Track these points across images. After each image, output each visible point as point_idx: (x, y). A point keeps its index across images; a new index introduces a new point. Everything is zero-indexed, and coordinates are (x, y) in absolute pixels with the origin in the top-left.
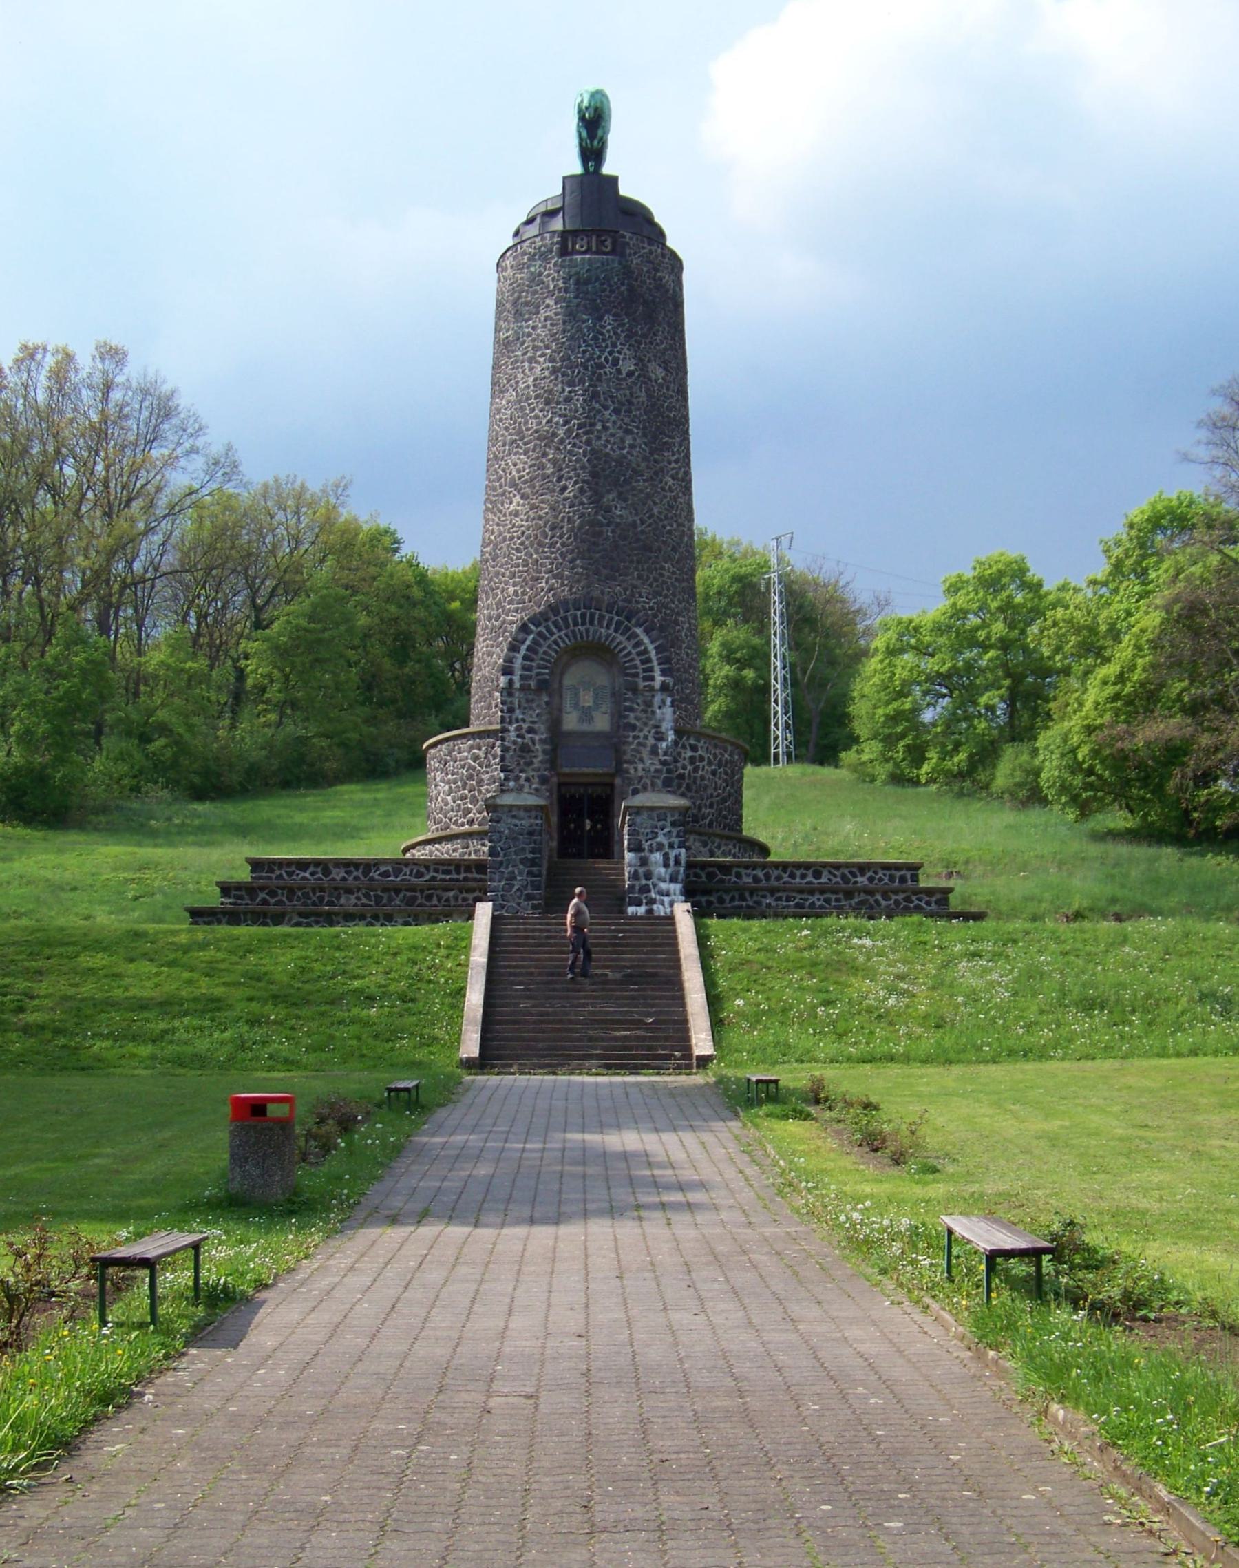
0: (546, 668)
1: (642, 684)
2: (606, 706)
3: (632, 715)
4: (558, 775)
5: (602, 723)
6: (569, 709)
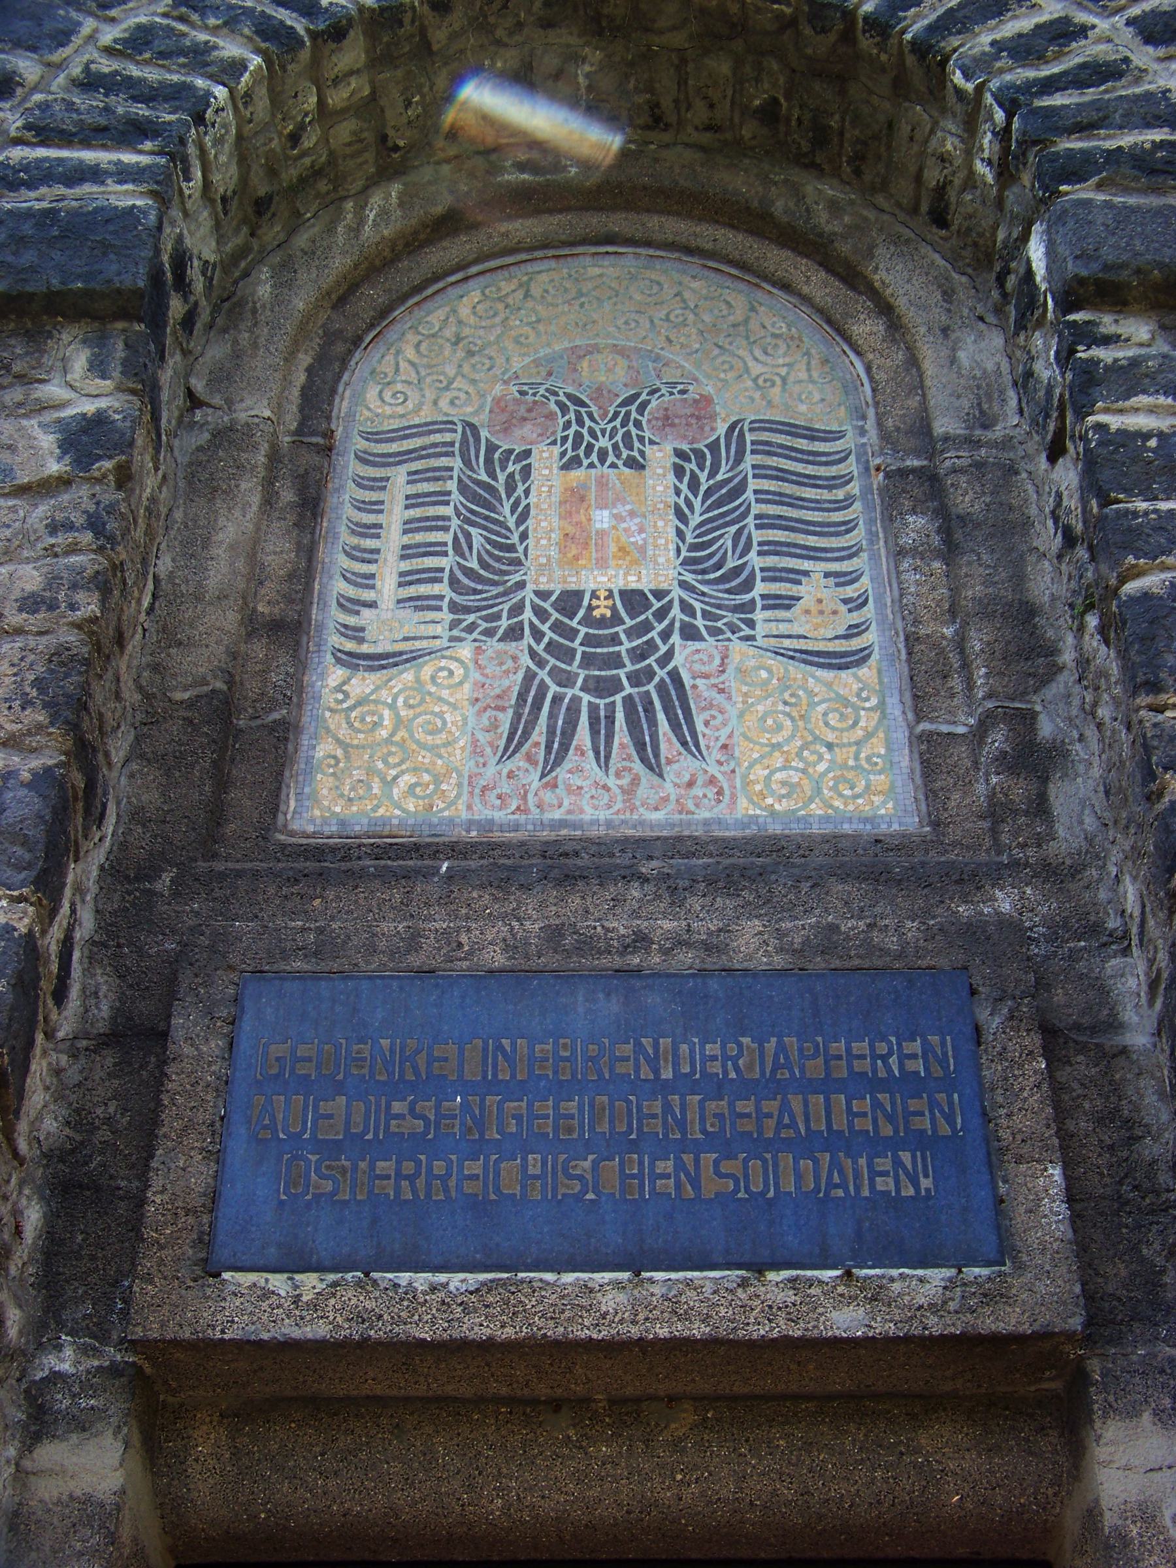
0: (133, 132)
2: (850, 588)
4: (168, 1390)
6: (386, 625)
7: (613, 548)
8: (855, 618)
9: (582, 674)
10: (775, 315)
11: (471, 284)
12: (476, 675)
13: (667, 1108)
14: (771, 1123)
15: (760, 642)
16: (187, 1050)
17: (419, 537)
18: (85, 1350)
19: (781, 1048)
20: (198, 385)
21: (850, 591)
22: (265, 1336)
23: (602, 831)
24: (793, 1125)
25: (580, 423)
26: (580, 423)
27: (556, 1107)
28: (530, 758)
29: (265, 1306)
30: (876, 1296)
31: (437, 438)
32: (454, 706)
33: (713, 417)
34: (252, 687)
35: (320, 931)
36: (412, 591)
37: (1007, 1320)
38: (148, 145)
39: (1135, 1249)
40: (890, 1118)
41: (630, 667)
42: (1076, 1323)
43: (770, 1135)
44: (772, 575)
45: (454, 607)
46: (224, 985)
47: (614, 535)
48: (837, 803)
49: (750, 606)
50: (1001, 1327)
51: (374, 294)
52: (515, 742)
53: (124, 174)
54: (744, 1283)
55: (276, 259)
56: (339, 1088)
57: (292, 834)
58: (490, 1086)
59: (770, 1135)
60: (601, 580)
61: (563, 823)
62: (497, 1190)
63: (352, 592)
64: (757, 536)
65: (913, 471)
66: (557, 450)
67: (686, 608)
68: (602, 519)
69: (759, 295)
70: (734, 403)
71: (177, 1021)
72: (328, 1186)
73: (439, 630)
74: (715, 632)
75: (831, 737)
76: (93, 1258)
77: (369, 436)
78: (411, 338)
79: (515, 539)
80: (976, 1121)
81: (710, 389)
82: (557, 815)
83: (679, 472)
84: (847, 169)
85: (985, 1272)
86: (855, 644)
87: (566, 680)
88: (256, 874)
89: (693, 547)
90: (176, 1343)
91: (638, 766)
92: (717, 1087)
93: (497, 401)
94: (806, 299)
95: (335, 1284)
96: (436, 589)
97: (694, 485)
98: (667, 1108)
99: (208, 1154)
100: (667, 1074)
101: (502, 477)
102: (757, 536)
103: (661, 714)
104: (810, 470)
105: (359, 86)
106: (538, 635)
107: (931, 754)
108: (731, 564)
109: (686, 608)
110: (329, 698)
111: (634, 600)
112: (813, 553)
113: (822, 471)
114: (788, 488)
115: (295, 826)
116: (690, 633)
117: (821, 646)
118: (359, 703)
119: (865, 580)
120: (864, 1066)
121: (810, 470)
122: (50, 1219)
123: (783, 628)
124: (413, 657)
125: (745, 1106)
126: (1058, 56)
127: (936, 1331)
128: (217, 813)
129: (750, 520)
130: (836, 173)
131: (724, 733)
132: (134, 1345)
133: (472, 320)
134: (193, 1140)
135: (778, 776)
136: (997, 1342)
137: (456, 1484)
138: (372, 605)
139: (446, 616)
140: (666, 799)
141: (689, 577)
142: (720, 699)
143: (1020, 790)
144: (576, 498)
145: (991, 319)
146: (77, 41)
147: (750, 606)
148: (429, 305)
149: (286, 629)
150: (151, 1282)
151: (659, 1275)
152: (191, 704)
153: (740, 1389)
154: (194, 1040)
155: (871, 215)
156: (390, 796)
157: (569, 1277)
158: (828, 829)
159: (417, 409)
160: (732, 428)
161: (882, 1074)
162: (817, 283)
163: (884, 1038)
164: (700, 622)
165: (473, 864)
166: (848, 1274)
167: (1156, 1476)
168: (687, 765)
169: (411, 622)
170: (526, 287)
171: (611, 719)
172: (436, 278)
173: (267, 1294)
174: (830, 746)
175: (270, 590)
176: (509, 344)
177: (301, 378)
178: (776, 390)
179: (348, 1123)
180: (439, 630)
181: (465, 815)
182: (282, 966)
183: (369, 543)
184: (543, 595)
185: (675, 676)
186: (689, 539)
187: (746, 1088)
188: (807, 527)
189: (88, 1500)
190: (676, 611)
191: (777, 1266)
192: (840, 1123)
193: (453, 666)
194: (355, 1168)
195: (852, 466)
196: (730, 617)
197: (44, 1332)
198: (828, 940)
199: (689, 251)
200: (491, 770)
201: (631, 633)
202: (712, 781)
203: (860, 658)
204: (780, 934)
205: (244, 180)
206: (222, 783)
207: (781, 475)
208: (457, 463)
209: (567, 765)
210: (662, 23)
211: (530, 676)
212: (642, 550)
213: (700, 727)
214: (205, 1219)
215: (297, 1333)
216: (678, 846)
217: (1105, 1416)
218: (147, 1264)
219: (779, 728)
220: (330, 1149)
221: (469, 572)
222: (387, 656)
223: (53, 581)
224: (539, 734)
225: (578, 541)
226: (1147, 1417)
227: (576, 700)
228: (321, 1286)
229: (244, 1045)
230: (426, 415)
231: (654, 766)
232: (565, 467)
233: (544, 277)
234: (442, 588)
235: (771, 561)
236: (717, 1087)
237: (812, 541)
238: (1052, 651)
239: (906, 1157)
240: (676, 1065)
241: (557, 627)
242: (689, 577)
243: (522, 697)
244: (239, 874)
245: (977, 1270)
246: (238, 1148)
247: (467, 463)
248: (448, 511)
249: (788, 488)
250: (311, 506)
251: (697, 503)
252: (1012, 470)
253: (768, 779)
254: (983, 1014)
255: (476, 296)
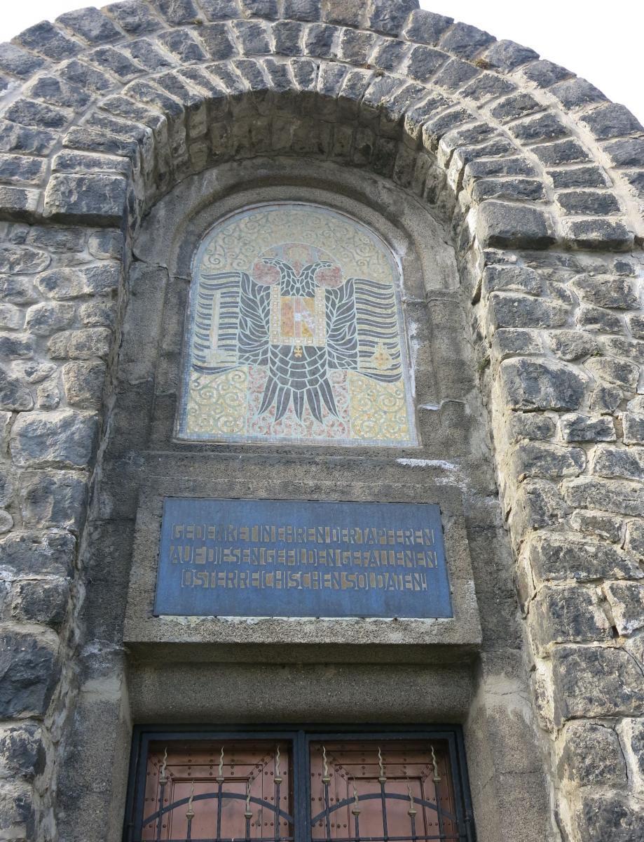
0: (113, 146)
1: (562, 224)
3: (543, 337)
5: (375, 411)
7: (302, 329)
8: (395, 362)
9: (291, 380)
10: (365, 235)
11: (245, 214)
12: (249, 378)
13: (328, 554)
14: (367, 561)
15: (359, 370)
16: (143, 527)
17: (226, 320)
18: (104, 645)
19: (371, 532)
20: (137, 252)
21: (393, 351)
22: (177, 641)
23: (299, 443)
24: (375, 562)
25: (289, 277)
26: (289, 277)
27: (287, 553)
28: (271, 413)
29: (176, 629)
30: (405, 628)
31: (232, 279)
32: (241, 390)
33: (341, 277)
34: (161, 379)
35: (195, 481)
36: (224, 342)
37: (456, 638)
38: (120, 152)
39: (499, 612)
40: (411, 560)
41: (309, 378)
42: (479, 640)
43: (366, 565)
44: (364, 343)
45: (241, 350)
46: (157, 502)
47: (303, 324)
48: (388, 435)
49: (354, 356)
50: (452, 642)
51: (206, 216)
52: (265, 406)
53: (111, 164)
54: (357, 623)
55: (167, 198)
56: (204, 544)
57: (178, 439)
58: (262, 544)
59: (366, 565)
60: (297, 342)
61: (285, 439)
62: (265, 585)
63: (200, 341)
64: (358, 327)
65: (418, 303)
66: (280, 287)
67: (330, 354)
68: (298, 317)
69: (359, 226)
70: (349, 272)
71: (139, 516)
72: (200, 582)
73: (234, 359)
74: (342, 365)
75: (385, 409)
76: (106, 608)
77: (205, 277)
78: (220, 235)
79: (264, 323)
80: (443, 562)
81: (339, 265)
82: (282, 435)
83: (328, 299)
84: (395, 177)
85: (446, 620)
86: (395, 372)
87: (284, 382)
88: (167, 457)
89: (334, 330)
90: (142, 643)
91: (312, 418)
92: (345, 546)
93: (256, 265)
94: (377, 229)
95: (204, 620)
96: (234, 342)
97: (333, 305)
98: (328, 554)
99: (153, 569)
100: (328, 541)
101: (258, 297)
102: (358, 327)
103: (320, 398)
104: (378, 301)
105: (203, 129)
106: (274, 363)
107: (423, 419)
108: (348, 337)
109: (330, 354)
110: (193, 385)
111: (311, 351)
112: (379, 335)
113: (383, 302)
114: (369, 308)
115: (181, 436)
116: (332, 365)
117: (382, 373)
118: (203, 388)
119: (399, 347)
120: (401, 540)
121: (378, 301)
122: (88, 591)
123: (368, 365)
124: (225, 370)
125: (357, 554)
126: (483, 140)
127: (428, 642)
128: (150, 430)
129: (355, 320)
130: (390, 177)
131: (345, 406)
132: (126, 644)
133: (245, 230)
134: (146, 563)
135: (366, 423)
136: (450, 646)
137: (245, 696)
138: (208, 347)
139: (237, 353)
140: (323, 431)
141: (332, 342)
142: (343, 392)
143: (458, 433)
144: (287, 308)
145: (450, 242)
146: (89, 103)
147: (354, 356)
148: (228, 222)
149: (176, 356)
150: (132, 619)
151: (327, 619)
152: (139, 386)
153: (352, 660)
154: (146, 523)
155: (404, 196)
156: (217, 425)
157: (292, 619)
158: (384, 445)
159: (225, 266)
160: (348, 282)
161: (408, 543)
162: (381, 223)
163: (408, 529)
164: (336, 361)
165: (251, 455)
166: (396, 619)
167: (505, 696)
168: (331, 417)
169: (224, 355)
170: (266, 217)
171: (302, 398)
172: (231, 211)
173: (178, 624)
174: (385, 412)
175: (168, 339)
176: (260, 241)
177: (177, 250)
178: (366, 267)
179: (207, 558)
180: (234, 359)
181: (246, 434)
182: (179, 495)
183: (206, 322)
184: (276, 347)
185: (326, 382)
186: (332, 327)
187: (358, 547)
188: (377, 324)
189: (107, 703)
190: (326, 356)
191: (370, 616)
192: (393, 562)
193: (241, 374)
194: (210, 575)
195: (394, 300)
196: (348, 359)
197: (90, 636)
198: (387, 491)
199: (331, 206)
200: (256, 417)
201: (310, 364)
202: (341, 424)
203: (396, 378)
204: (370, 488)
205: (156, 166)
206: (152, 419)
207: (367, 302)
208: (240, 290)
209: (285, 416)
210: (326, 111)
211: (270, 380)
212: (314, 330)
213: (336, 403)
214: (152, 594)
215: (189, 640)
216: (330, 450)
217: (488, 675)
218: (129, 612)
219: (366, 404)
220: (201, 568)
221: (246, 336)
222: (215, 369)
223: (89, 337)
224: (274, 403)
225: (288, 327)
226: (503, 674)
227: (288, 390)
228: (198, 621)
229: (166, 526)
230: (227, 270)
231: (319, 417)
232: (283, 295)
233: (274, 213)
234: (235, 342)
235: (363, 337)
236: (345, 546)
237: (379, 330)
238: (471, 380)
239: (417, 575)
240: (331, 537)
241: (282, 361)
242: (332, 342)
243: (267, 388)
244: (161, 456)
245: (443, 620)
246: (164, 566)
247: (245, 290)
248: (237, 310)
249: (369, 308)
250: (183, 303)
251: (335, 312)
252: (457, 305)
253: (362, 424)
254: (445, 522)
255: (247, 219)
